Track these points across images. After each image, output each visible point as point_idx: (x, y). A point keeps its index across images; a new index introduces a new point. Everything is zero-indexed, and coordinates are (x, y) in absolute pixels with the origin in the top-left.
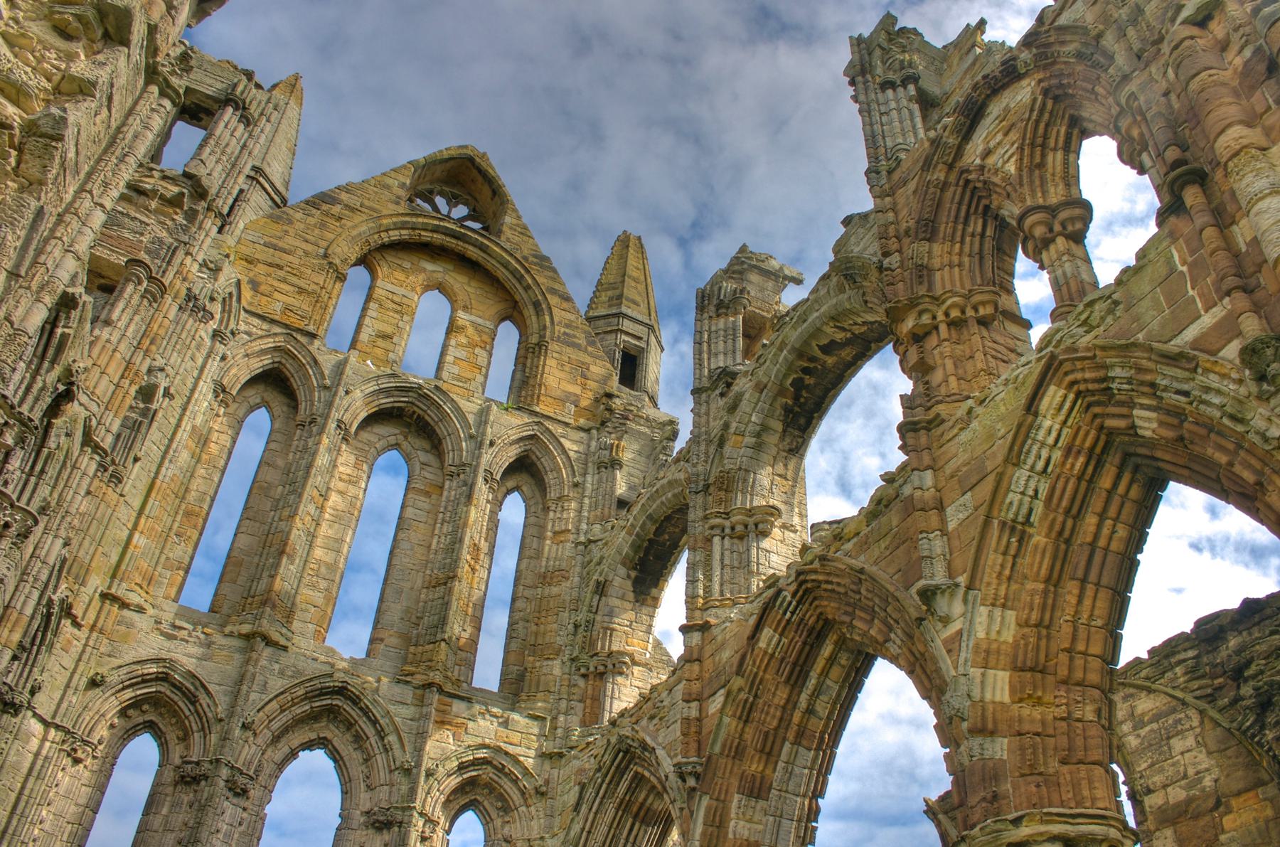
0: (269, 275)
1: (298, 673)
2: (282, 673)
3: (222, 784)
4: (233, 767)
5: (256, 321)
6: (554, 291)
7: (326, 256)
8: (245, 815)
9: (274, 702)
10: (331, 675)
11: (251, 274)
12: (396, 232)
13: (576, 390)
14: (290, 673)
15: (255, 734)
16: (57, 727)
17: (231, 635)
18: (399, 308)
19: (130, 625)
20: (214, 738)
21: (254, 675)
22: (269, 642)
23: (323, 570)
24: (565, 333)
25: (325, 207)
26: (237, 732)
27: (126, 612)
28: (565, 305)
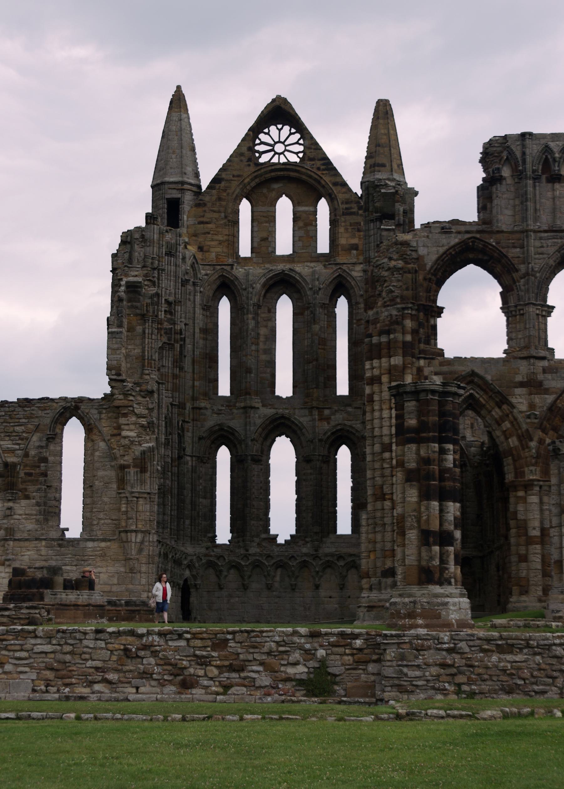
2: (259, 417)
3: (249, 461)
6: (335, 184)
7: (226, 217)
13: (355, 241)
15: (257, 441)
17: (238, 409)
18: (267, 219)
19: (205, 415)
20: (243, 446)
21: (250, 422)
24: (346, 209)
25: (217, 186)
26: (250, 443)
27: (202, 411)
28: (344, 190)
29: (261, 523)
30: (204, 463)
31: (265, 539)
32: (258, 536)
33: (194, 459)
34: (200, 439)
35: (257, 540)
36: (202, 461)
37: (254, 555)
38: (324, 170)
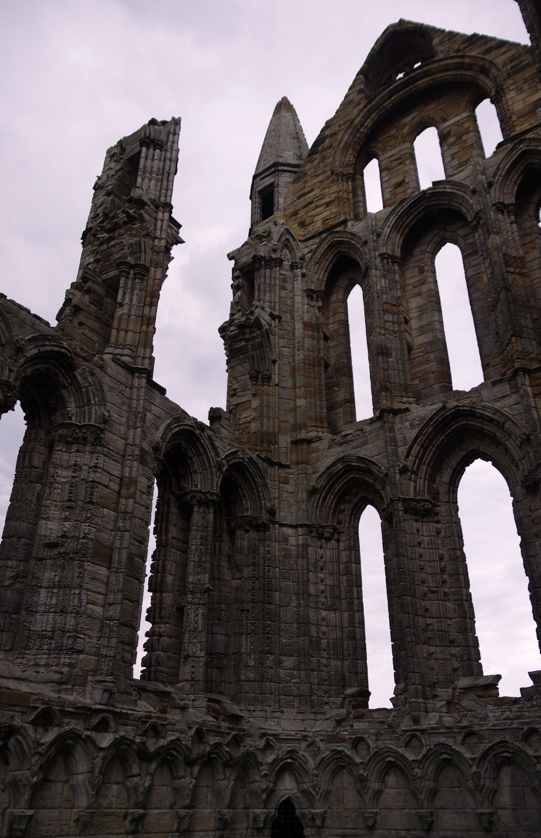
0: (307, 212)
1: (422, 419)
2: (412, 426)
4: (404, 500)
5: (311, 242)
6: (489, 51)
8: (439, 526)
9: (415, 446)
10: (444, 408)
11: (298, 220)
12: (369, 120)
14: (417, 423)
16: (301, 526)
18: (400, 161)
19: (318, 450)
22: (397, 412)
23: (428, 348)
25: (320, 148)
27: (313, 445)
29: (453, 650)
30: (328, 539)
31: (467, 690)
32: (449, 682)
33: (300, 529)
34: (313, 492)
35: (444, 693)
36: (320, 537)
37: (433, 731)
38: (467, 47)
